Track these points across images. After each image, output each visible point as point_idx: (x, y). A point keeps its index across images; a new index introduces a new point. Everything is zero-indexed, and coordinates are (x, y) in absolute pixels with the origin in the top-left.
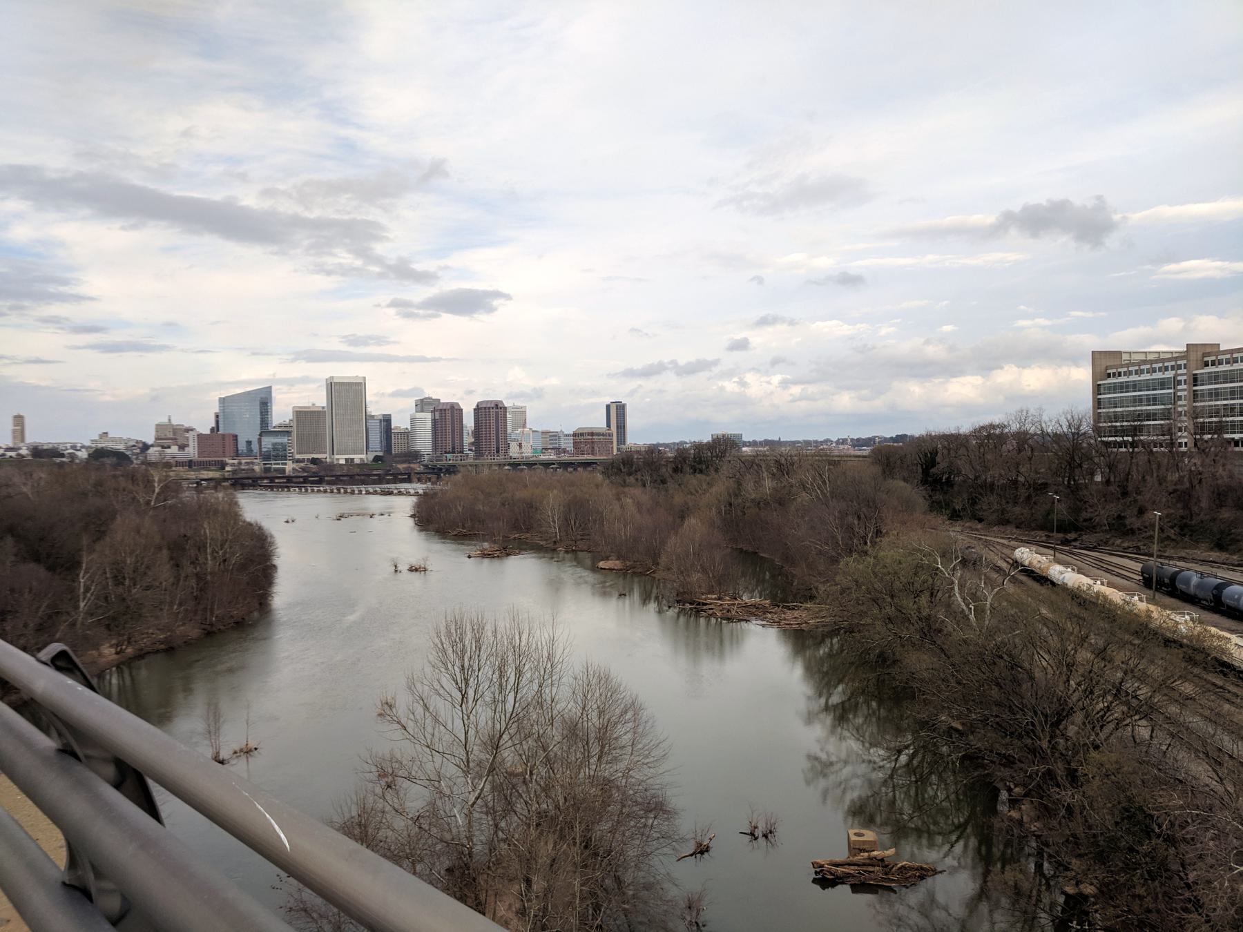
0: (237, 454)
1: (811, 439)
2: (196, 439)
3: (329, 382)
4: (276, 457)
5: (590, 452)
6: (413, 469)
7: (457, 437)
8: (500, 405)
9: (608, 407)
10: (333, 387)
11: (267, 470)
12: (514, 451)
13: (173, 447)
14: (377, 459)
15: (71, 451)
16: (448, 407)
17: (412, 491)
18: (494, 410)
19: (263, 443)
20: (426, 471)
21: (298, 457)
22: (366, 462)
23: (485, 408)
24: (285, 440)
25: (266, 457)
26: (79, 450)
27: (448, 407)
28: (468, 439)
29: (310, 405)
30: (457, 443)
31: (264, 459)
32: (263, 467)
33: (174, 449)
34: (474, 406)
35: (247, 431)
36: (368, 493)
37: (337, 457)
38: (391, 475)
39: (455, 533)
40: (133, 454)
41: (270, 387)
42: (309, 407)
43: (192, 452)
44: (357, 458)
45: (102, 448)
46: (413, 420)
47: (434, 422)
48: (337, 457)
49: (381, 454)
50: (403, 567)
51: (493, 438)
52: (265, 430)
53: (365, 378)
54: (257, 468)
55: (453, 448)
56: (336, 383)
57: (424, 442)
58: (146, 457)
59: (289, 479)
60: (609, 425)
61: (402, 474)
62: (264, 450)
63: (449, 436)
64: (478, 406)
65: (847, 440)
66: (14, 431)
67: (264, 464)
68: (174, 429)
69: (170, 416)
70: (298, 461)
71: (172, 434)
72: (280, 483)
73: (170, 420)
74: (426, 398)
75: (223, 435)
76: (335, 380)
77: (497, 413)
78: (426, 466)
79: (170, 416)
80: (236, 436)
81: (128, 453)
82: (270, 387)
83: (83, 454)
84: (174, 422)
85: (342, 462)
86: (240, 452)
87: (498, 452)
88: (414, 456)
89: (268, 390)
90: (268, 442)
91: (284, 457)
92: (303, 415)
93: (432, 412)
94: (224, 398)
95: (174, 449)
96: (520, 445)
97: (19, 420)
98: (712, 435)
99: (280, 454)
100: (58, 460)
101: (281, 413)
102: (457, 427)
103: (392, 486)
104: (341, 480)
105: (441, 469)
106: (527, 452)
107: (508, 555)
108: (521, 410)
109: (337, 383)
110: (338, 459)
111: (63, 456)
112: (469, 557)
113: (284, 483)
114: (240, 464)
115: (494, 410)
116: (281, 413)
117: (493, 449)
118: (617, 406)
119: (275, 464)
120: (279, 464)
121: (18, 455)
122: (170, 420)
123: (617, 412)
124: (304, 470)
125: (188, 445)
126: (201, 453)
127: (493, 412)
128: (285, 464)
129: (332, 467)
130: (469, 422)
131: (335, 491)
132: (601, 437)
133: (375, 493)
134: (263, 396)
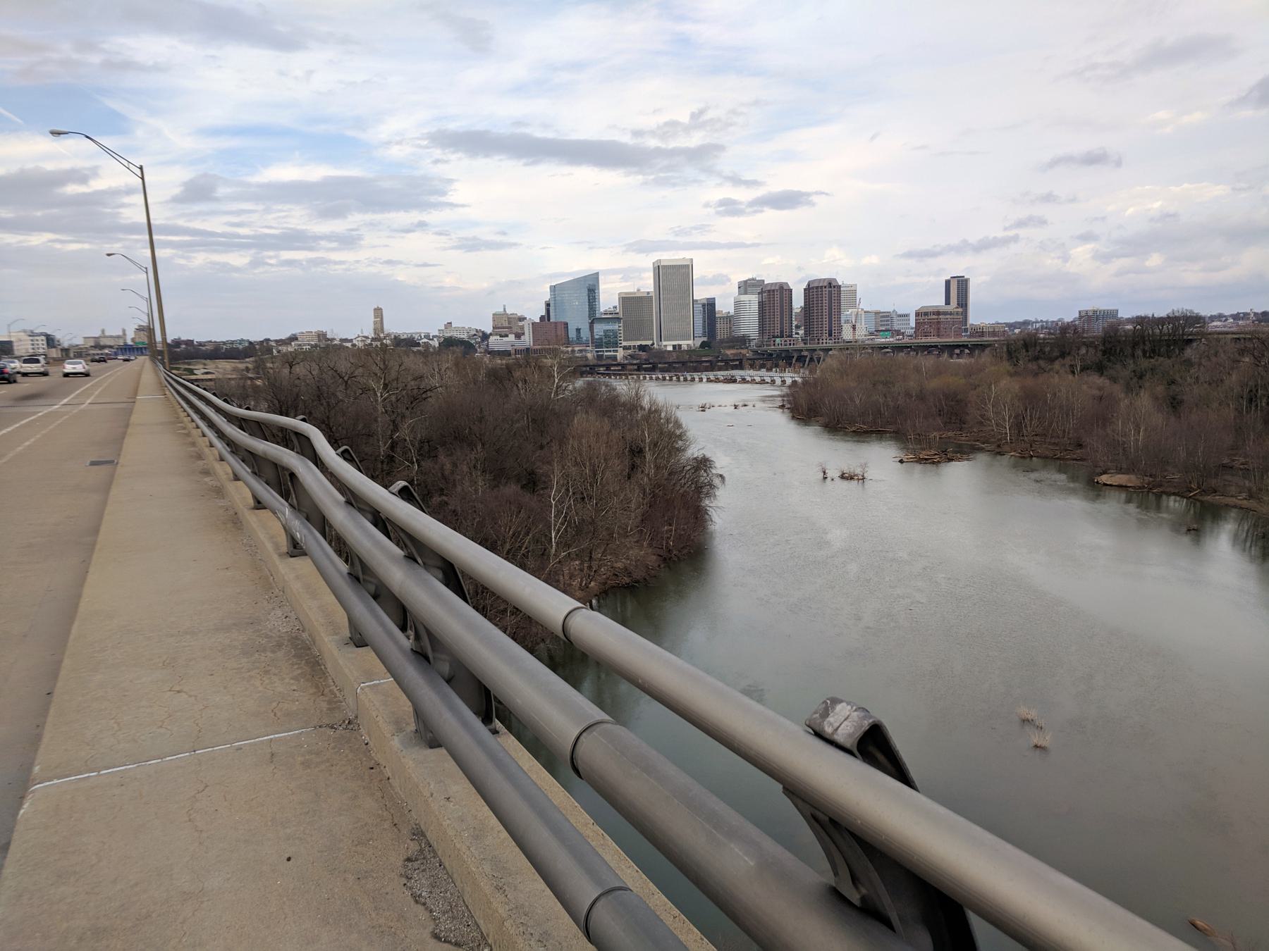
0: (568, 343)
3: (656, 265)
4: (608, 345)
5: (935, 334)
6: (744, 355)
7: (786, 319)
8: (834, 284)
9: (948, 283)
10: (659, 270)
11: (600, 357)
12: (847, 334)
13: (510, 335)
14: (703, 345)
15: (426, 340)
16: (777, 288)
17: (758, 379)
18: (827, 289)
19: (595, 331)
20: (755, 357)
21: (624, 344)
22: (693, 348)
23: (817, 288)
24: (616, 327)
25: (598, 344)
26: (432, 339)
27: (777, 288)
29: (636, 291)
30: (786, 327)
31: (597, 347)
32: (595, 355)
33: (512, 337)
34: (805, 285)
35: (577, 320)
36: (709, 380)
37: (664, 343)
38: (722, 361)
39: (854, 429)
40: (476, 343)
41: (597, 273)
42: (634, 293)
43: (528, 340)
44: (685, 344)
45: (451, 337)
46: (738, 304)
47: (762, 305)
48: (664, 343)
49: (705, 339)
50: (833, 473)
51: (826, 320)
52: (594, 320)
53: (692, 259)
54: (589, 355)
55: (782, 332)
57: (749, 326)
58: (488, 346)
59: (623, 366)
60: (948, 302)
61: (734, 360)
62: (597, 337)
63: (778, 319)
64: (809, 285)
65: (1249, 314)
66: (375, 323)
67: (598, 352)
68: (509, 318)
69: (504, 306)
70: (625, 348)
71: (507, 323)
72: (615, 370)
73: (505, 309)
74: (749, 280)
75: (556, 323)
77: (830, 293)
78: (755, 352)
79: (504, 306)
81: (473, 342)
82: (597, 273)
83: (436, 343)
84: (509, 312)
85: (670, 348)
86: (571, 339)
88: (743, 341)
89: (595, 277)
90: (600, 329)
91: (616, 344)
92: (630, 302)
93: (759, 293)
95: (512, 337)
96: (854, 327)
97: (378, 312)
98: (1080, 312)
99: (611, 341)
100: (415, 349)
101: (608, 299)
102: (786, 307)
103: (738, 374)
104: (674, 368)
105: (771, 355)
106: (861, 333)
107: (950, 460)
108: (852, 289)
109: (664, 267)
110: (666, 346)
111: (418, 344)
112: (901, 461)
113: (619, 370)
114: (573, 351)
115: (827, 289)
116: (608, 299)
118: (958, 281)
119: (607, 351)
120: (610, 351)
121: (382, 344)
122: (505, 309)
123: (959, 288)
124: (632, 356)
125: (523, 334)
128: (617, 351)
129: (662, 353)
130: (798, 302)
131: (674, 378)
132: (947, 317)
133: (717, 381)
134: (591, 283)
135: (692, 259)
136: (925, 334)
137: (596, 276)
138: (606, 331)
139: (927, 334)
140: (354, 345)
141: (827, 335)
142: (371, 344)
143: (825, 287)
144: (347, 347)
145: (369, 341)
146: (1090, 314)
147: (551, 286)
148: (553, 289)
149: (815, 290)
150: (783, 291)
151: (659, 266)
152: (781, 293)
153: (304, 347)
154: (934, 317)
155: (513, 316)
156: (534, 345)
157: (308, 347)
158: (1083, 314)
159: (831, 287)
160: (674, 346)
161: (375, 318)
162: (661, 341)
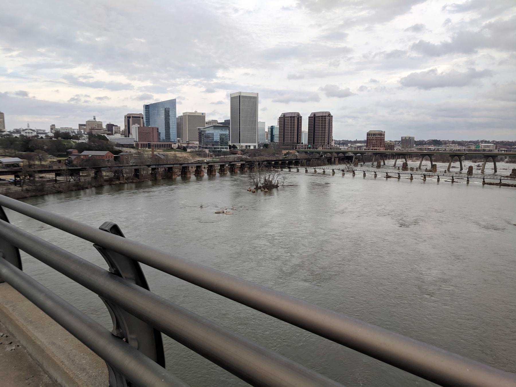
1: (467, 140)
2: (137, 130)
37: (242, 144)
41: (175, 100)
48: (242, 144)
53: (258, 94)
56: (242, 96)
68: (98, 124)
73: (95, 119)
76: (242, 95)
80: (158, 129)
82: (175, 100)
87: (328, 144)
94: (147, 106)
98: (402, 137)
115: (328, 118)
117: (326, 142)
120: (223, 148)
121: (47, 136)
126: (140, 138)
127: (327, 118)
136: (373, 145)
140: (22, 136)
142: (37, 136)
143: (327, 116)
144: (16, 137)
145: (35, 134)
146: (408, 138)
148: (147, 107)
149: (321, 118)
150: (298, 118)
151: (240, 96)
152: (298, 118)
155: (100, 123)
156: (139, 141)
158: (403, 138)
159: (330, 117)
160: (246, 146)
162: (240, 143)
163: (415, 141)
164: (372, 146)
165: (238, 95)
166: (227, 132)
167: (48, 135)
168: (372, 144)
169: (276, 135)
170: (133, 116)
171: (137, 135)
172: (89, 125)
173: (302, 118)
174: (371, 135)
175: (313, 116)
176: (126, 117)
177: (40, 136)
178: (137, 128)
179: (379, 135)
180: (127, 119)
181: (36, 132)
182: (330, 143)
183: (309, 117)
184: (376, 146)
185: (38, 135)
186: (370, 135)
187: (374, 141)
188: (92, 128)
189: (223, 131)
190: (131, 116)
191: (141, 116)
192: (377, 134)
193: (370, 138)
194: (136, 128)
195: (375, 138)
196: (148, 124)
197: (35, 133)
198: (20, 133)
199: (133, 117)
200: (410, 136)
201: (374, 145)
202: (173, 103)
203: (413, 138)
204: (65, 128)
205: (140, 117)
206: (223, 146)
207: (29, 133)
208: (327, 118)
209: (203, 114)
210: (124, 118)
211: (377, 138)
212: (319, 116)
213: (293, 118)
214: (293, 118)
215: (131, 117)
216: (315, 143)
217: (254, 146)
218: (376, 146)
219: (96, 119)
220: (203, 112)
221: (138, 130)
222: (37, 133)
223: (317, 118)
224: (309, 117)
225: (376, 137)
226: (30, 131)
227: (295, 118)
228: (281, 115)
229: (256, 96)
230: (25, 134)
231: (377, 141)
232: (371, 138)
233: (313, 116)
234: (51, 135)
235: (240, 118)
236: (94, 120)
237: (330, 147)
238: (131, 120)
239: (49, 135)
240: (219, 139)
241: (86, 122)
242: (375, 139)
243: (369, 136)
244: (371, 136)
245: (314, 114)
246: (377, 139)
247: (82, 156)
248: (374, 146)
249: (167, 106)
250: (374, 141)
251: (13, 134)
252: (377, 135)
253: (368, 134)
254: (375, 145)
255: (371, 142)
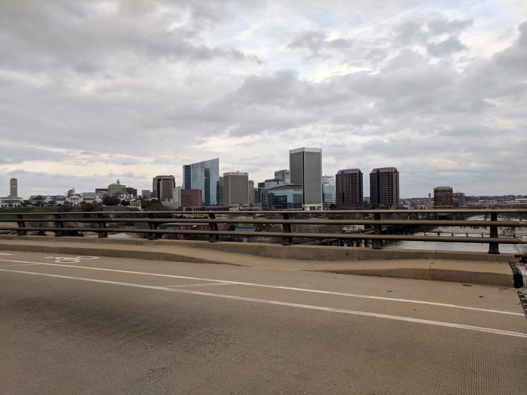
2: (180, 193)
27: (357, 172)
28: (366, 193)
41: (218, 159)
53: (321, 149)
56: (306, 152)
68: (122, 188)
73: (118, 182)
76: (306, 150)
82: (218, 159)
84: (121, 184)
87: (397, 203)
97: (14, 182)
109: (308, 153)
121: (95, 202)
127: (394, 175)
135: (321, 149)
136: (443, 203)
137: (217, 160)
138: (295, 196)
139: (446, 203)
140: (66, 203)
141: (395, 202)
144: (60, 205)
145: (81, 200)
147: (183, 166)
149: (387, 174)
151: (303, 152)
153: (14, 204)
154: (449, 193)
155: (124, 187)
157: (17, 204)
161: (11, 185)
163: (466, 197)
164: (442, 204)
165: (301, 151)
166: (301, 192)
167: (96, 201)
168: (441, 201)
169: (327, 194)
170: (164, 178)
171: (180, 198)
172: (112, 189)
173: (398, 173)
174: (440, 192)
175: (376, 172)
176: (155, 180)
177: (87, 202)
178: (180, 191)
179: (449, 192)
180: (156, 181)
181: (82, 198)
182: (398, 202)
183: (370, 174)
184: (446, 203)
185: (85, 202)
186: (438, 192)
187: (444, 199)
188: (118, 192)
189: (296, 191)
190: (162, 178)
191: (172, 178)
192: (447, 190)
193: (439, 195)
194: (179, 190)
195: (445, 195)
196: (189, 186)
197: (81, 199)
198: (65, 200)
199: (163, 179)
200: (461, 192)
201: (444, 203)
202: (216, 162)
203: (464, 194)
204: (89, 193)
205: (171, 179)
206: (297, 208)
207: (75, 199)
208: (394, 174)
209: (246, 174)
210: (152, 181)
211: (447, 194)
212: (348, 174)
213: (354, 175)
214: (354, 175)
215: (162, 180)
216: (380, 202)
217: (310, 207)
218: (447, 204)
219: (120, 183)
220: (245, 172)
221: (181, 193)
222: (84, 199)
223: (381, 175)
224: (370, 174)
225: (446, 193)
226: (77, 197)
227: (357, 175)
228: (338, 173)
229: (320, 152)
230: (70, 201)
231: (447, 198)
232: (440, 195)
233: (376, 172)
234: (100, 201)
235: (304, 176)
236: (118, 184)
237: (398, 206)
238: (161, 183)
239: (97, 201)
240: (292, 200)
241: (109, 186)
242: (445, 197)
243: (437, 193)
244: (440, 193)
245: (378, 171)
246: (447, 196)
247: (182, 227)
248: (444, 204)
249: (208, 166)
250: (444, 199)
251: (57, 202)
252: (447, 192)
253: (436, 191)
254: (445, 202)
255: (440, 199)
